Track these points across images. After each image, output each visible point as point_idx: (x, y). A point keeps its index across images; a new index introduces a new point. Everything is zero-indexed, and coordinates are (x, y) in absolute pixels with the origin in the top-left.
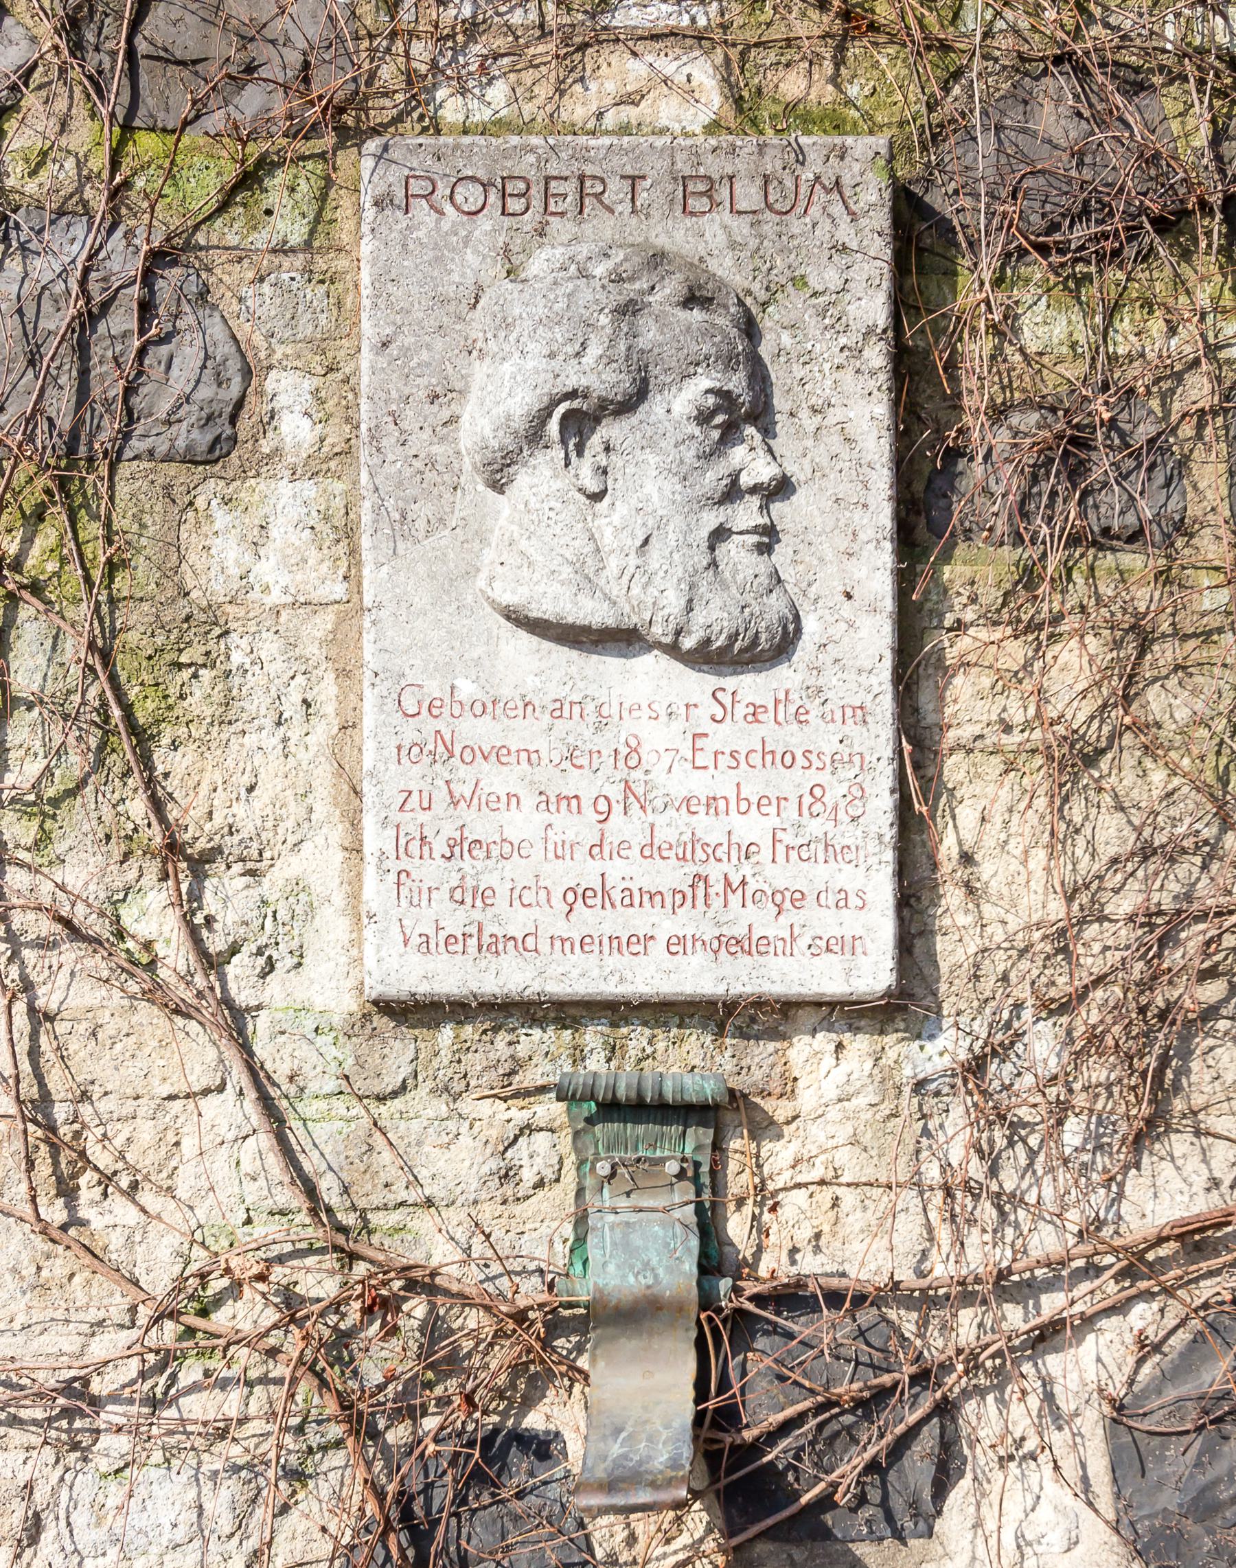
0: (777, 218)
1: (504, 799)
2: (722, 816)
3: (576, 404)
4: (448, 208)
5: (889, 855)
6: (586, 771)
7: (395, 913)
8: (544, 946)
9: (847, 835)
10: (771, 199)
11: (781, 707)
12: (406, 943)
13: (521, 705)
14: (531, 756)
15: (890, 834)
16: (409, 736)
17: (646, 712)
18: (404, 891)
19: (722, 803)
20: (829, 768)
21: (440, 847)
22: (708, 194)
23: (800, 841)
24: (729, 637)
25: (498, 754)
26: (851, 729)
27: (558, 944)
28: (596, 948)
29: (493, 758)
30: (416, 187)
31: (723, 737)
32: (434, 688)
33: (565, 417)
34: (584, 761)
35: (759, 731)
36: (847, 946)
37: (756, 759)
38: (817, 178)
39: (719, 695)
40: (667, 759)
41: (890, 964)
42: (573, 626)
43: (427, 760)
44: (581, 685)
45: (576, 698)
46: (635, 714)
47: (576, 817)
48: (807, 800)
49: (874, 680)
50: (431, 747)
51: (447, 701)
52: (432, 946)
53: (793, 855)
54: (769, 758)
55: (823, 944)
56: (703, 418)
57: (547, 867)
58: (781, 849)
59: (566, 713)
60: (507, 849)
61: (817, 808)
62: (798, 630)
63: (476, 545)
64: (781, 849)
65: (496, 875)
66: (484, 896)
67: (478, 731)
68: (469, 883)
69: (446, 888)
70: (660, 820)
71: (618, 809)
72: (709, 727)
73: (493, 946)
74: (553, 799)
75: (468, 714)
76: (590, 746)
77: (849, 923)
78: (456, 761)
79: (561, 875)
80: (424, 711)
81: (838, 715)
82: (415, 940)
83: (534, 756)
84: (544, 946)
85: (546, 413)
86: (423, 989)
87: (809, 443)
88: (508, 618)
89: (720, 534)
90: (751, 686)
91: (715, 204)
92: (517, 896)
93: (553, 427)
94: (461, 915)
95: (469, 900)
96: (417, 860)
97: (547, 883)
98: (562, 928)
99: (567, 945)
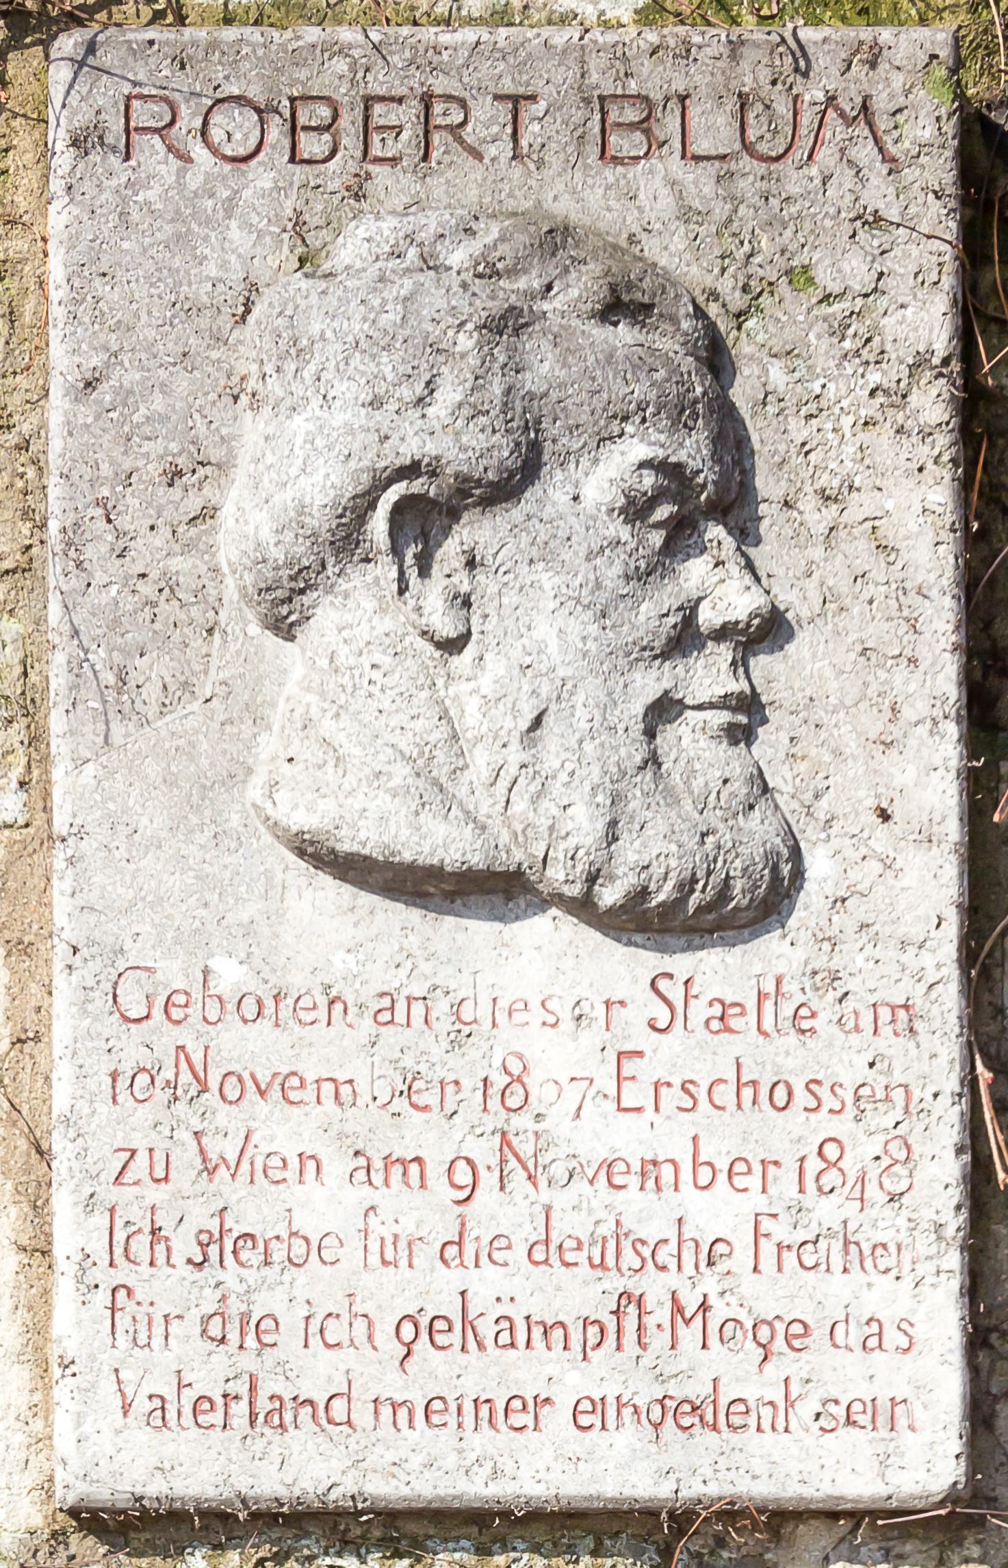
0: (761, 168)
1: (294, 1163)
2: (668, 1192)
3: (417, 486)
4: (199, 151)
5: (954, 1260)
6: (435, 1115)
7: (108, 1358)
8: (363, 1417)
9: (884, 1225)
10: (752, 135)
11: (768, 1006)
12: (126, 1409)
13: (322, 1002)
14: (340, 1090)
15: (954, 1223)
16: (132, 1055)
17: (537, 1014)
18: (123, 1321)
19: (667, 1171)
20: (850, 1111)
21: (184, 1245)
22: (643, 126)
24: (680, 886)
25: (284, 1087)
26: (888, 1043)
27: (386, 1411)
28: (452, 1420)
29: (276, 1093)
30: (143, 114)
31: (669, 1056)
32: (174, 973)
33: (398, 510)
34: (431, 1098)
35: (731, 1046)
36: (883, 1415)
37: (725, 1095)
38: (831, 99)
39: (663, 985)
41: (956, 1446)
42: (411, 868)
44: (425, 967)
46: (519, 1017)
47: (418, 1196)
48: (814, 1165)
49: (927, 960)
50: (169, 1074)
51: (197, 995)
52: (171, 1415)
53: (790, 1258)
54: (747, 1093)
55: (840, 1412)
56: (635, 510)
57: (368, 1280)
59: (400, 1017)
60: (299, 1248)
62: (798, 874)
63: (247, 729)
65: (281, 1294)
66: (260, 1329)
68: (235, 1307)
69: (194, 1315)
70: (561, 1199)
71: (489, 1180)
73: (275, 1416)
74: (378, 1164)
75: (232, 1017)
76: (440, 1073)
77: (886, 1376)
78: (212, 1098)
79: (393, 1294)
80: (158, 1013)
82: (142, 1405)
83: (345, 1090)
84: (363, 1417)
85: (366, 502)
86: (155, 1489)
87: (817, 553)
88: (301, 853)
89: (664, 709)
90: (717, 969)
91: (655, 144)
92: (315, 1330)
93: (378, 525)
94: (221, 1363)
96: (144, 1268)
98: (393, 1385)
99: (403, 1413)
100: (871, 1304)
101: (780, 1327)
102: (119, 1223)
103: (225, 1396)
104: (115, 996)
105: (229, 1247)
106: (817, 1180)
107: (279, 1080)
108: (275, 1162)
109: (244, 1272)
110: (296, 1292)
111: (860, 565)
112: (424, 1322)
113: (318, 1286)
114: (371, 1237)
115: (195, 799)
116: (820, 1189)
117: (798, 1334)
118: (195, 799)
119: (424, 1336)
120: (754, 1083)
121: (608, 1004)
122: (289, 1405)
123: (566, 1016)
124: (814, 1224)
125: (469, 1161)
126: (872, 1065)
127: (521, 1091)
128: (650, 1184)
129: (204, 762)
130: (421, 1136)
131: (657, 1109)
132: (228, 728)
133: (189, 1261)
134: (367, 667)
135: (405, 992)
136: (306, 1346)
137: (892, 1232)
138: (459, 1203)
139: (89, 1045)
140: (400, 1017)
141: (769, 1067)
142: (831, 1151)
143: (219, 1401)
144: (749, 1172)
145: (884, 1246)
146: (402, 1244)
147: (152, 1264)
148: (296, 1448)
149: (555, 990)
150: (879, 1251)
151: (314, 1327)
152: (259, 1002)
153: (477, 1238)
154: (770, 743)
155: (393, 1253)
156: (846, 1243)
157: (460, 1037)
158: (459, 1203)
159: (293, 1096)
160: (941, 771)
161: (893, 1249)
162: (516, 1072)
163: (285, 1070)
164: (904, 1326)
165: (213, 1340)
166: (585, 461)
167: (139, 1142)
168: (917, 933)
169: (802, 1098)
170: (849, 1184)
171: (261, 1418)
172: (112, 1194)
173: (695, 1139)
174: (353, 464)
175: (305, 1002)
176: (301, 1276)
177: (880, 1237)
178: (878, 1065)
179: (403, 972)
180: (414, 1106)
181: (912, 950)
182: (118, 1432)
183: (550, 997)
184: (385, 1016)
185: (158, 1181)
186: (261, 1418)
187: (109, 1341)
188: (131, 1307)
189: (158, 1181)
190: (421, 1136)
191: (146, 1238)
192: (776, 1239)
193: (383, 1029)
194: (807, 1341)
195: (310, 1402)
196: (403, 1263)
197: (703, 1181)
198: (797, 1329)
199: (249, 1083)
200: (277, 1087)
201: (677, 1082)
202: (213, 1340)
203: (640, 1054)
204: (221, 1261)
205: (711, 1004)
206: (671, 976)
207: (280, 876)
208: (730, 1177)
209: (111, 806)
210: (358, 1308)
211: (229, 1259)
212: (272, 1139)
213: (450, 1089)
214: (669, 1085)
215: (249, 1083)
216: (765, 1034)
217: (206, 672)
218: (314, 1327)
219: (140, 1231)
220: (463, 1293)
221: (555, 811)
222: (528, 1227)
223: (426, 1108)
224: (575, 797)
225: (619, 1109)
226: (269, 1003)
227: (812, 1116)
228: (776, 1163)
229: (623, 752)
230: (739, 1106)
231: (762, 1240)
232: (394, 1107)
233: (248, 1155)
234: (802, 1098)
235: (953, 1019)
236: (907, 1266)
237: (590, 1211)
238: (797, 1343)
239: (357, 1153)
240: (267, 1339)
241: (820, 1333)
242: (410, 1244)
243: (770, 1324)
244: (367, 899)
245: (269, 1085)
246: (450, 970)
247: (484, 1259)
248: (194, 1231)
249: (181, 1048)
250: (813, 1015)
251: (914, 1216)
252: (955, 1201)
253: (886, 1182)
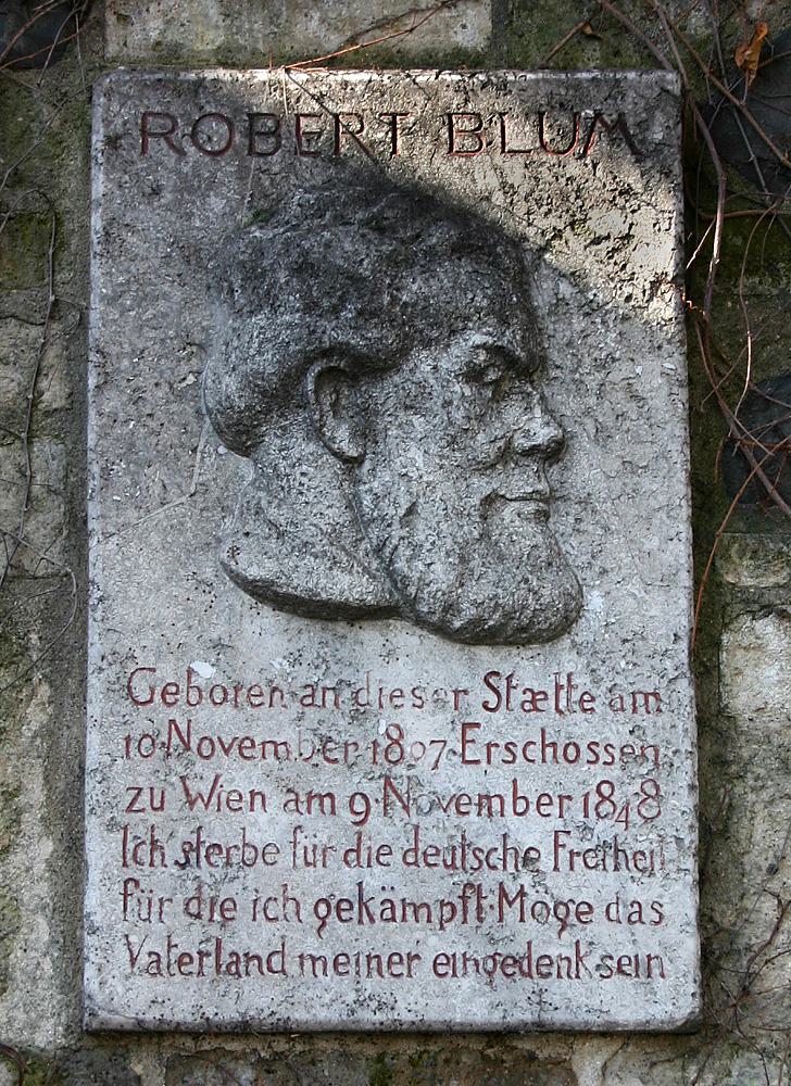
0: (553, 159)
1: (247, 797)
5: (690, 863)
6: (340, 767)
7: (122, 927)
8: (293, 969)
9: (641, 839)
10: (546, 137)
11: (563, 694)
12: (133, 961)
13: (266, 690)
15: (691, 838)
16: (141, 725)
17: (408, 700)
18: (132, 903)
19: (496, 803)
21: (174, 852)
23: (587, 845)
25: (242, 747)
26: (642, 718)
27: (308, 964)
28: (352, 969)
29: (235, 751)
30: (153, 124)
31: (497, 726)
32: (168, 672)
34: (338, 755)
35: (539, 720)
36: (642, 968)
37: (535, 752)
38: (598, 115)
40: (433, 752)
41: (692, 988)
43: (159, 753)
44: (334, 668)
45: (329, 683)
46: (397, 701)
47: (330, 820)
48: (594, 799)
49: (668, 664)
50: (164, 739)
51: (183, 686)
52: (163, 966)
53: (578, 861)
54: (549, 750)
55: (613, 964)
56: (473, 375)
57: (296, 875)
58: (563, 854)
59: (319, 702)
61: (606, 808)
64: (563, 854)
65: (237, 885)
66: (225, 910)
67: (219, 720)
68: (207, 893)
69: (180, 898)
70: (425, 822)
71: (376, 808)
72: (481, 716)
73: (236, 966)
74: (303, 798)
75: (206, 701)
77: (647, 941)
79: (312, 884)
80: (157, 698)
81: (628, 701)
82: (144, 960)
83: (281, 749)
84: (293, 969)
87: (592, 401)
89: (490, 500)
90: (528, 669)
95: (206, 914)
97: (297, 893)
98: (312, 946)
99: (319, 964)
100: (634, 892)
101: (572, 907)
102: (130, 837)
105: (203, 853)
106: (596, 809)
107: (237, 742)
108: (235, 796)
109: (213, 870)
112: (333, 903)
114: (298, 847)
115: (183, 558)
116: (598, 814)
117: (584, 912)
118: (183, 558)
119: (334, 913)
120: (554, 744)
121: (456, 692)
124: (595, 839)
125: (364, 796)
126: (631, 732)
130: (328, 779)
131: (489, 762)
133: (177, 863)
134: (298, 476)
135: (321, 685)
136: (254, 919)
137: (647, 844)
140: (319, 702)
141: (563, 734)
142: (606, 789)
144: (551, 804)
146: (319, 851)
147: (152, 864)
148: (246, 988)
150: (639, 856)
153: (369, 848)
154: (562, 523)
156: (617, 850)
158: (356, 823)
160: (675, 541)
163: (241, 735)
165: (191, 915)
167: (142, 782)
168: (662, 645)
169: (586, 755)
170: (618, 811)
171: (223, 968)
172: (123, 818)
173: (515, 781)
177: (639, 847)
178: (636, 733)
179: (320, 672)
180: (327, 759)
184: (309, 700)
186: (223, 968)
188: (137, 893)
190: (328, 779)
191: (147, 847)
192: (568, 848)
193: (306, 709)
194: (589, 916)
196: (319, 864)
197: (520, 809)
198: (584, 908)
199: (217, 745)
200: (235, 747)
201: (502, 743)
202: (191, 915)
203: (478, 725)
204: (198, 862)
205: (524, 693)
209: (128, 564)
210: (290, 894)
211: (203, 861)
212: (233, 780)
213: (351, 748)
214: (497, 745)
215: (217, 745)
217: (191, 477)
219: (143, 842)
222: (403, 839)
227: (592, 766)
228: (569, 798)
229: (466, 528)
230: (544, 761)
232: (315, 759)
233: (216, 792)
234: (586, 755)
236: (657, 866)
237: (445, 829)
239: (289, 791)
240: (228, 915)
241: (599, 911)
242: (324, 851)
243: (566, 905)
244: (298, 623)
245: (231, 746)
246: (351, 670)
247: (374, 861)
248: (179, 843)
249: (172, 721)
251: (662, 833)
252: (689, 822)
253: (643, 811)
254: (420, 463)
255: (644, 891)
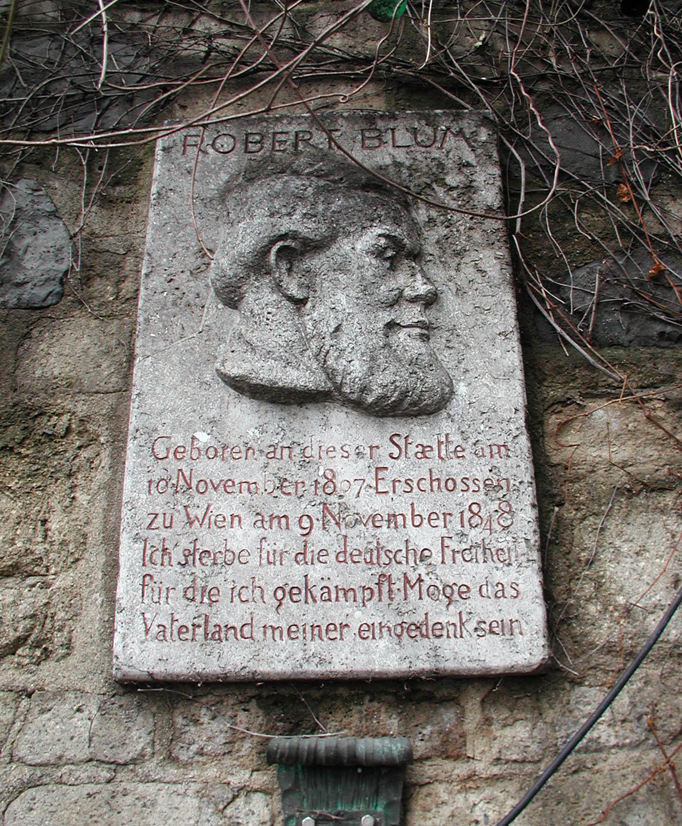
1: (229, 519)
2: (401, 529)
3: (287, 243)
4: (211, 150)
5: (535, 555)
6: (293, 497)
7: (140, 608)
8: (258, 635)
9: (503, 541)
11: (443, 447)
12: (147, 631)
13: (243, 449)
14: (251, 487)
15: (534, 538)
16: (158, 473)
17: (339, 453)
18: (148, 590)
19: (400, 519)
20: (482, 491)
21: (177, 556)
22: (379, 138)
23: (464, 546)
24: (401, 393)
25: (226, 486)
26: (497, 461)
27: (269, 632)
28: (300, 635)
29: (221, 488)
31: (398, 469)
32: (178, 439)
33: (279, 251)
34: (291, 490)
35: (427, 464)
36: (506, 629)
37: (425, 485)
38: (448, 129)
39: (395, 439)
40: (356, 487)
41: (542, 641)
42: (282, 389)
43: (170, 491)
44: (289, 434)
45: (285, 444)
46: (331, 454)
47: (285, 533)
48: (467, 515)
49: (512, 427)
50: (174, 482)
51: (188, 448)
52: (168, 634)
53: (459, 557)
54: (435, 484)
55: (486, 627)
56: (379, 253)
57: (261, 571)
58: (448, 552)
59: (278, 456)
60: (230, 557)
61: (476, 520)
62: (452, 392)
63: (216, 343)
64: (448, 552)
65: (221, 578)
66: (210, 594)
67: (211, 469)
68: (200, 583)
69: (180, 587)
70: (352, 533)
71: (317, 525)
72: (388, 462)
73: (215, 634)
74: (267, 519)
75: (203, 457)
76: (296, 478)
77: (508, 610)
78: (193, 491)
79: (272, 577)
80: (171, 456)
81: (487, 451)
82: (155, 630)
83: (253, 486)
84: (258, 635)
85: (264, 252)
86: (159, 670)
87: (453, 273)
88: (236, 388)
89: (391, 326)
90: (420, 433)
91: (382, 143)
92: (236, 593)
93: (272, 257)
94: (192, 609)
95: (198, 598)
96: (158, 567)
97: (262, 583)
98: (272, 619)
99: (277, 632)
100: (498, 576)
101: (455, 588)
102: (148, 546)
103: (193, 625)
104: (153, 449)
105: (197, 557)
106: (469, 521)
107: (223, 483)
108: (220, 518)
109: (204, 568)
110: (227, 577)
111: (470, 277)
112: (287, 589)
113: (235, 574)
114: (264, 551)
115: (192, 370)
116: (471, 525)
117: (464, 592)
118: (192, 370)
119: (288, 596)
120: (438, 479)
121: (371, 447)
122: (224, 629)
123: (353, 453)
124: (469, 541)
125: (309, 517)
126: (491, 471)
127: (332, 486)
128: (392, 525)
129: (197, 355)
130: (284, 505)
131: (394, 492)
132: (208, 343)
133: (179, 563)
134: (266, 313)
135: (280, 445)
136: (232, 602)
137: (505, 544)
138: (304, 535)
139: (140, 469)
140: (278, 456)
141: (444, 473)
142: (475, 508)
143: (191, 627)
144: (438, 518)
145: (502, 550)
146: (277, 555)
147: (162, 565)
148: (226, 650)
149: (347, 442)
150: (500, 552)
151: (236, 593)
152: (216, 449)
153: (312, 551)
154: (438, 341)
155: (275, 558)
156: (485, 549)
157: (305, 463)
158: (304, 535)
159: (229, 490)
160: (511, 352)
161: (506, 550)
162: (330, 477)
163: (226, 478)
164: (514, 586)
165: (189, 599)
166: (357, 236)
167: (158, 510)
168: (507, 416)
169: (460, 486)
170: (484, 522)
171: (210, 636)
172: (145, 534)
173: (412, 504)
174: (261, 236)
175: (236, 450)
176: (230, 570)
177: (500, 546)
178: (494, 471)
179: (279, 437)
180: (284, 493)
181: (505, 423)
182: (142, 642)
183: (345, 445)
184: (272, 455)
185: (166, 527)
186: (210, 636)
187: (140, 600)
188: (152, 584)
189: (166, 527)
190: (284, 505)
191: (159, 553)
192: (451, 548)
193: (270, 461)
194: (468, 594)
195: (233, 628)
196: (278, 563)
197: (417, 523)
198: (464, 589)
199: (210, 485)
200: (222, 486)
201: (403, 480)
202: (189, 599)
203: (386, 468)
204: (194, 563)
205: (417, 447)
206: (398, 435)
207: (227, 398)
208: (429, 521)
209: (157, 373)
210: (257, 584)
211: (197, 562)
212: (219, 508)
213: (300, 485)
214: (399, 481)
215: (210, 485)
216: (442, 459)
217: (200, 322)
218: (236, 593)
219: (157, 550)
220: (306, 576)
221: (345, 363)
222: (336, 545)
223: (289, 494)
224: (354, 357)
225: (378, 492)
226: (220, 450)
227: (465, 493)
228: (450, 514)
229: (374, 341)
230: (432, 490)
231: (446, 549)
232: (275, 493)
233: (208, 516)
234: (460, 486)
235: (525, 450)
236: (513, 559)
237: (365, 537)
238: (464, 596)
239: (258, 514)
240: (214, 599)
241: (474, 591)
242: (281, 554)
243: (451, 587)
244: (266, 407)
245: (218, 485)
246: (300, 435)
247: (316, 561)
248: (182, 550)
249: (181, 470)
250: (463, 450)
251: (515, 536)
252: (533, 529)
253: (501, 522)
254: (344, 302)
255: (504, 576)
